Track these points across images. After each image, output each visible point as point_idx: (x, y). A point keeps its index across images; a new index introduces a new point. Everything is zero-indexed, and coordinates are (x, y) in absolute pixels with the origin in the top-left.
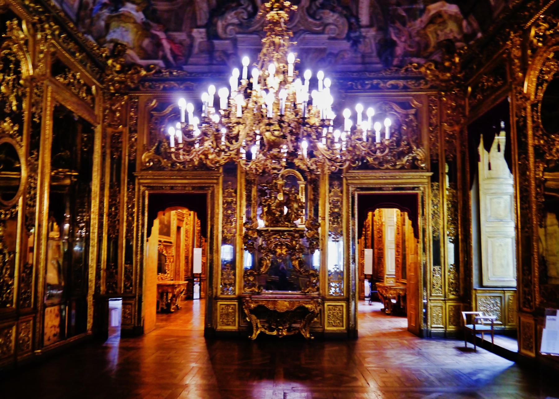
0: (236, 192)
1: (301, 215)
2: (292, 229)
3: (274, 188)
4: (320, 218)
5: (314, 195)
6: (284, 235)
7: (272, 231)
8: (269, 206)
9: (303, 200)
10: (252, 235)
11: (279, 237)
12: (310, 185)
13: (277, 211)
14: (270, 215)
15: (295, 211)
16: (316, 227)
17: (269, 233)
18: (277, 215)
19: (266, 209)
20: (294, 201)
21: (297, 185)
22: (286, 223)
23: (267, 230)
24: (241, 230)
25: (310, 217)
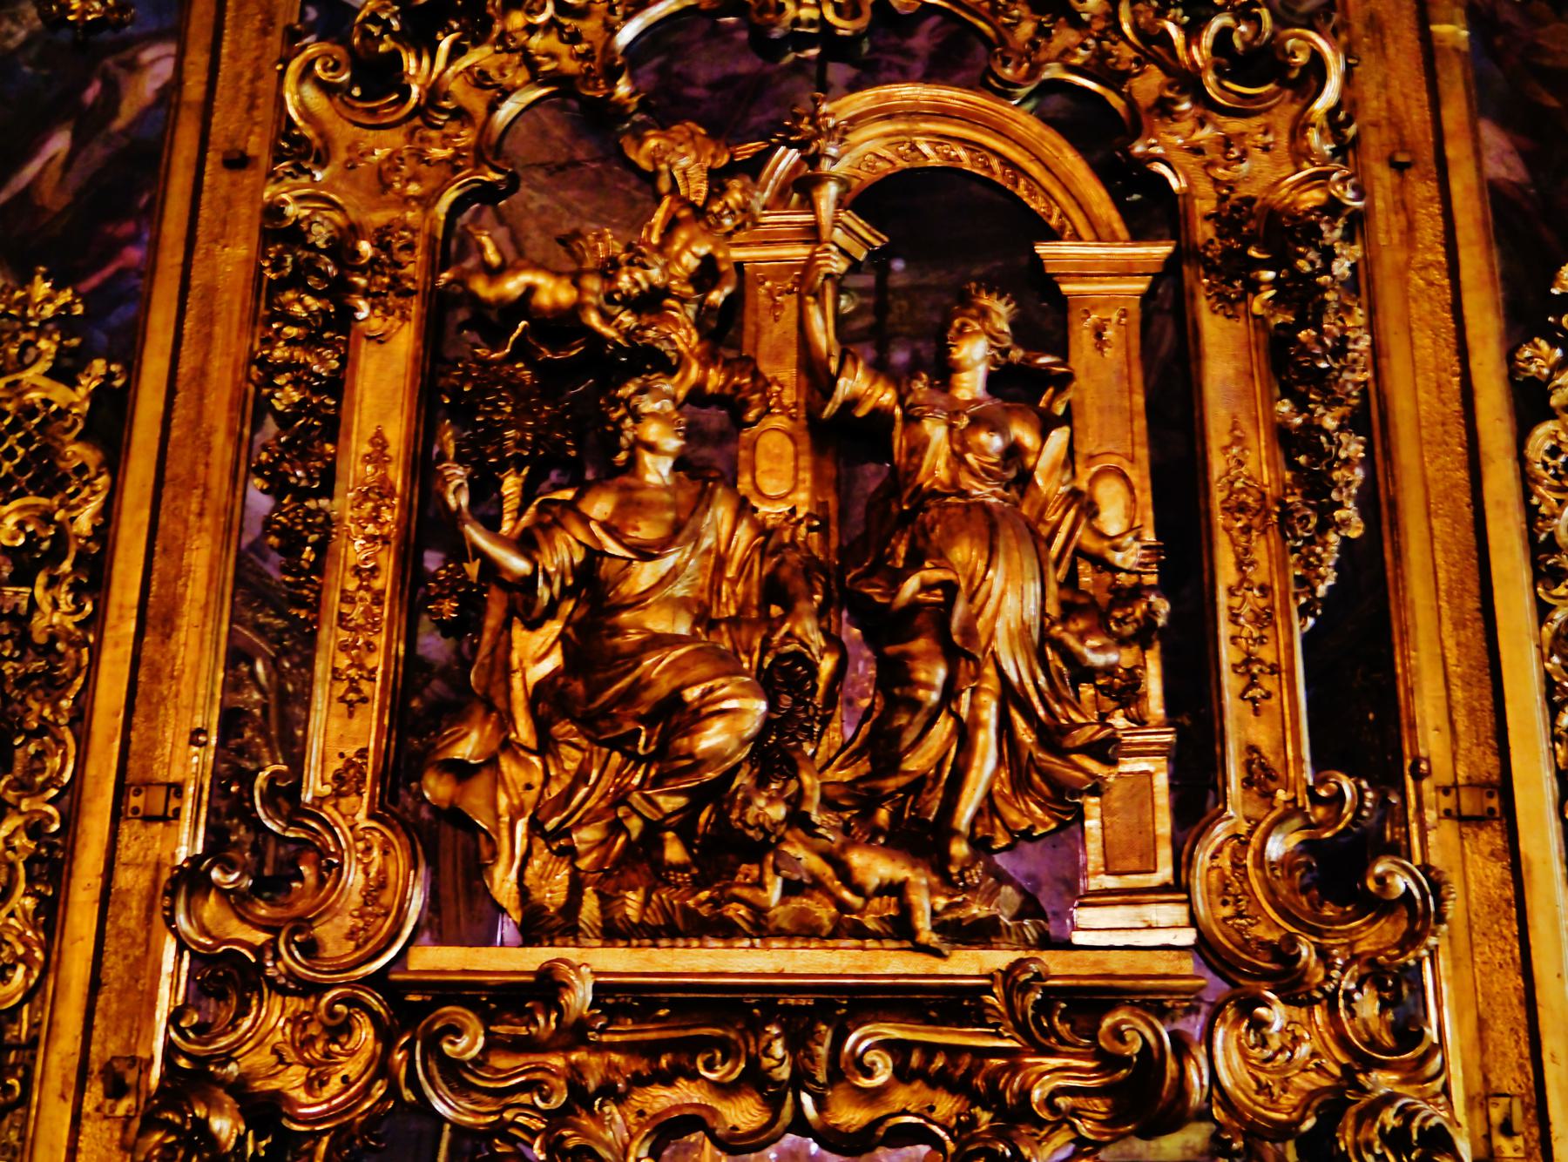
0: (109, 421)
1: (1108, 750)
2: (968, 964)
3: (683, 337)
4: (1427, 801)
5: (1286, 440)
6: (844, 1070)
7: (616, 997)
8: (592, 584)
9: (1122, 516)
10: (292, 1081)
11: (743, 1114)
12: (1229, 306)
13: (727, 664)
14: (596, 726)
15: (1015, 666)
16: (1374, 936)
17: (574, 1034)
18: (713, 737)
19: (537, 655)
20: (989, 528)
21: (1045, 313)
22: (874, 867)
23: (548, 985)
24: (117, 988)
25: (1260, 778)
